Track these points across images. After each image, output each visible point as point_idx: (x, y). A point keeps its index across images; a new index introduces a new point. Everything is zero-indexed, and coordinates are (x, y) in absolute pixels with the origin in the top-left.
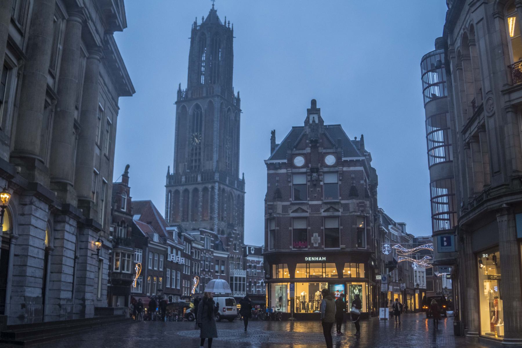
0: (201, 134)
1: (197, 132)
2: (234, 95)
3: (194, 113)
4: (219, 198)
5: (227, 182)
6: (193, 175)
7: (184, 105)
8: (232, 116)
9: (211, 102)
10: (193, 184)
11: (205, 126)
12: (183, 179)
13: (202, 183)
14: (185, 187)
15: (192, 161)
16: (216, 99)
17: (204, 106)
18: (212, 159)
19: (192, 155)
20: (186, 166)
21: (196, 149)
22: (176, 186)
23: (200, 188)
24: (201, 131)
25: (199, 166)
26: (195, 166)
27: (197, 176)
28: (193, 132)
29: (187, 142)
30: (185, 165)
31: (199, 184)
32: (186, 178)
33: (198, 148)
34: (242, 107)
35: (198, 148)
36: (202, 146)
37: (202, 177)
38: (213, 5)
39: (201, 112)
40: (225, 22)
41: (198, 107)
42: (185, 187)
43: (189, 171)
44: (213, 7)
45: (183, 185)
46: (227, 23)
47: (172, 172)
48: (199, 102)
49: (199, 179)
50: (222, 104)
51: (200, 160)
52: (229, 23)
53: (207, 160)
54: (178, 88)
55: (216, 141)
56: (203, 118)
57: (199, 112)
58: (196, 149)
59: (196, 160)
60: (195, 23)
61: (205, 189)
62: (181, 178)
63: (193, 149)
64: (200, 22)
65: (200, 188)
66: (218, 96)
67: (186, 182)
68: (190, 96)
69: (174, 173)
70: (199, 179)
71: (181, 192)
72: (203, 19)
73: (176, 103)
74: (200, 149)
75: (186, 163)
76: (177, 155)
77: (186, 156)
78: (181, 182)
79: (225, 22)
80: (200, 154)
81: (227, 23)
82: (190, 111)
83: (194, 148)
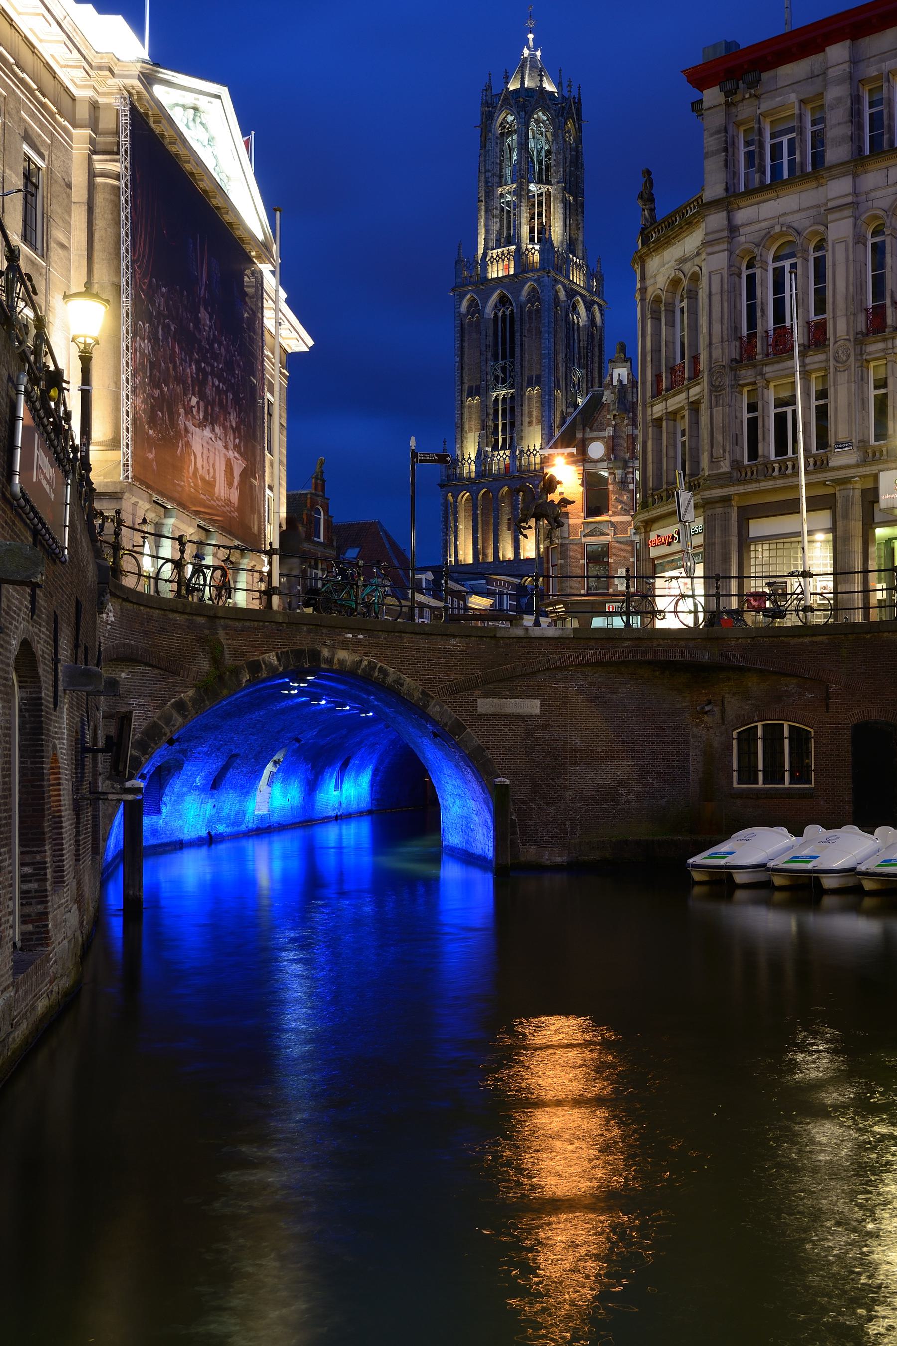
0: (512, 363)
1: (504, 358)
3: (496, 315)
11: (522, 345)
24: (512, 355)
56: (517, 327)
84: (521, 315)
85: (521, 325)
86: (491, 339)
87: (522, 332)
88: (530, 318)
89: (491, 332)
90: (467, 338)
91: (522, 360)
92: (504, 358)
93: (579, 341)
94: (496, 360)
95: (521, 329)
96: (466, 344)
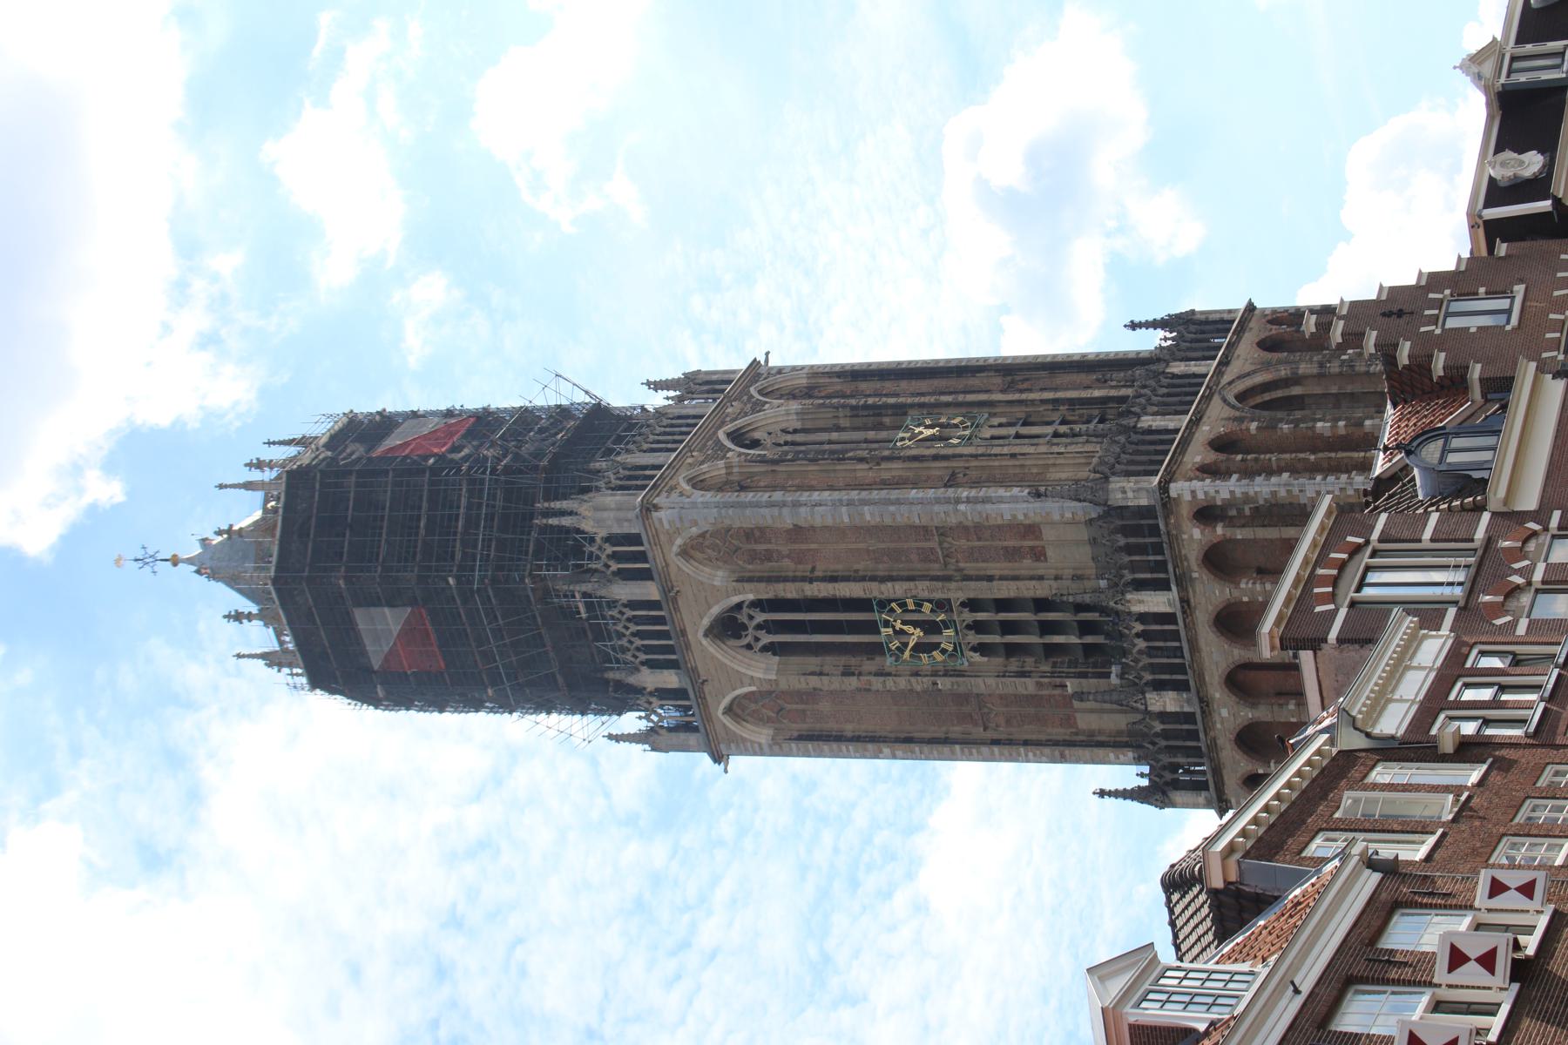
0: (883, 604)
1: (872, 628)
2: (660, 413)
3: (771, 648)
4: (1270, 472)
5: (1169, 422)
6: (1141, 644)
7: (729, 710)
8: (779, 415)
9: (684, 553)
10: (1194, 648)
11: (833, 579)
12: (1168, 702)
13: (1183, 582)
14: (1217, 693)
15: (1051, 650)
16: (663, 516)
17: (710, 589)
18: (1031, 530)
19: (1011, 650)
20: (1091, 684)
21: (978, 627)
22: (1213, 746)
23: (1211, 594)
24: (863, 604)
25: (1080, 608)
26: (1086, 628)
27: (1143, 618)
28: (877, 649)
29: (944, 683)
30: (1080, 696)
31: (1185, 602)
32: (1159, 686)
33: (969, 617)
34: (730, 359)
35: (969, 617)
36: (957, 593)
37: (1140, 585)
38: (175, 561)
39: (758, 604)
40: (248, 486)
41: (728, 627)
42: (1217, 693)
43: (1115, 669)
44: (190, 561)
45: (1205, 702)
46: (256, 475)
47: (1129, 775)
48: (696, 621)
49: (1157, 602)
50: (698, 483)
51: (1041, 604)
52: (259, 465)
53: (1039, 555)
54: (637, 748)
55: (921, 505)
56: (790, 591)
57: (761, 617)
58: (978, 627)
59: (1047, 628)
60: (272, 659)
61: (1218, 561)
62: (1163, 716)
63: (982, 649)
64: (261, 637)
65: (1211, 594)
66: (648, 509)
67: (1181, 687)
68: (670, 679)
69: (1138, 761)
70: (1157, 602)
71: (1247, 714)
72: (238, 617)
73: (718, 758)
74: (973, 605)
75: (1071, 685)
76: (1026, 743)
77: (1028, 686)
78: (1189, 718)
79: (248, 486)
80: (1003, 605)
81: (256, 475)
82: (757, 670)
83: (973, 638)
84: (760, 580)
85: (786, 580)
86: (830, 662)
87: (803, 579)
88: (768, 556)
89: (813, 662)
90: (832, 726)
91: (873, 579)
92: (872, 628)
93: (838, 429)
94: (877, 649)
95: (794, 579)
96: (849, 729)
